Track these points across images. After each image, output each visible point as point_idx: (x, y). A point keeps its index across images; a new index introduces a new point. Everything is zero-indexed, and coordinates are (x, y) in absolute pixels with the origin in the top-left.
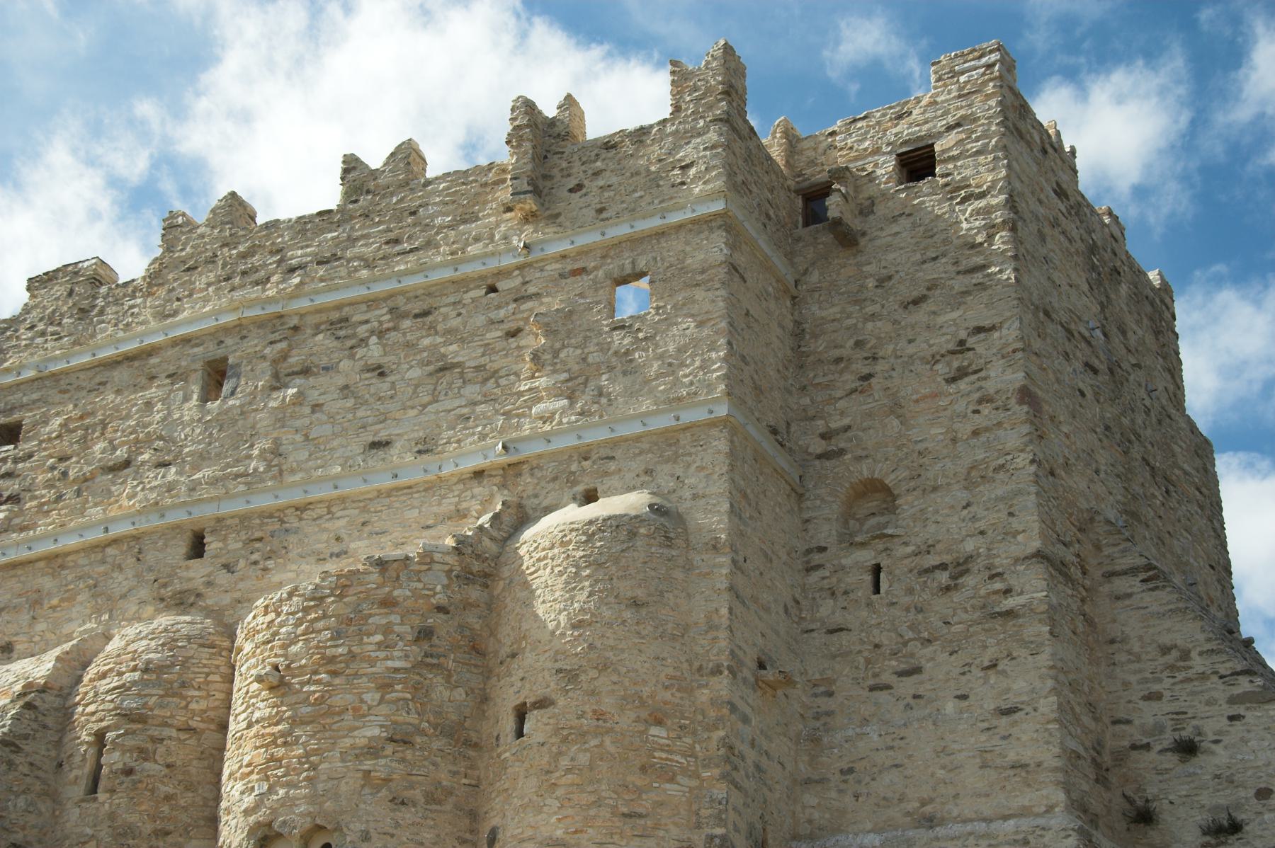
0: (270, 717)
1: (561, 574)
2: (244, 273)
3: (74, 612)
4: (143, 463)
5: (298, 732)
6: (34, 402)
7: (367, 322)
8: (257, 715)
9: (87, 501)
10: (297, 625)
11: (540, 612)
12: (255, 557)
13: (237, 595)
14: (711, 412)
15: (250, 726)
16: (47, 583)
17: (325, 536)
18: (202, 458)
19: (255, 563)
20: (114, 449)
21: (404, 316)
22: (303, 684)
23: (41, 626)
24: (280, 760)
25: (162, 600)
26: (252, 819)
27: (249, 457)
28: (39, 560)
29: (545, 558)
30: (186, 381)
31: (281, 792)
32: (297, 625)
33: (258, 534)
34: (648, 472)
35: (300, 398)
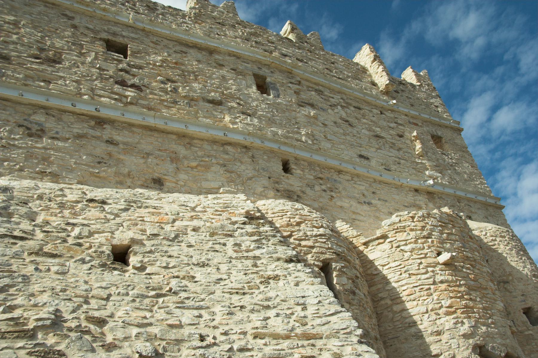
0: (452, 281)
1: (511, 250)
2: (256, 42)
3: (209, 176)
4: (232, 107)
5: (474, 294)
6: (133, 38)
7: (333, 98)
8: (439, 278)
9: (197, 112)
10: (441, 233)
11: (513, 264)
12: (324, 187)
13: (321, 205)
14: (496, 202)
15: (434, 283)
16: (182, 151)
17: (356, 191)
18: (271, 122)
19: (324, 191)
20: (209, 92)
21: (350, 105)
22: (463, 267)
23: (182, 176)
24: (472, 308)
25: (278, 191)
26: (471, 341)
27: (300, 133)
28: (172, 133)
29: (495, 240)
30: (244, 76)
31: (484, 328)
32: (441, 233)
33: (320, 175)
34: (487, 218)
35: (315, 117)
